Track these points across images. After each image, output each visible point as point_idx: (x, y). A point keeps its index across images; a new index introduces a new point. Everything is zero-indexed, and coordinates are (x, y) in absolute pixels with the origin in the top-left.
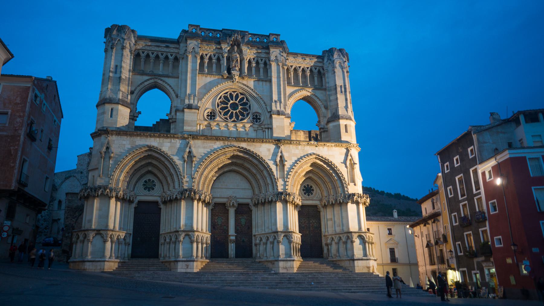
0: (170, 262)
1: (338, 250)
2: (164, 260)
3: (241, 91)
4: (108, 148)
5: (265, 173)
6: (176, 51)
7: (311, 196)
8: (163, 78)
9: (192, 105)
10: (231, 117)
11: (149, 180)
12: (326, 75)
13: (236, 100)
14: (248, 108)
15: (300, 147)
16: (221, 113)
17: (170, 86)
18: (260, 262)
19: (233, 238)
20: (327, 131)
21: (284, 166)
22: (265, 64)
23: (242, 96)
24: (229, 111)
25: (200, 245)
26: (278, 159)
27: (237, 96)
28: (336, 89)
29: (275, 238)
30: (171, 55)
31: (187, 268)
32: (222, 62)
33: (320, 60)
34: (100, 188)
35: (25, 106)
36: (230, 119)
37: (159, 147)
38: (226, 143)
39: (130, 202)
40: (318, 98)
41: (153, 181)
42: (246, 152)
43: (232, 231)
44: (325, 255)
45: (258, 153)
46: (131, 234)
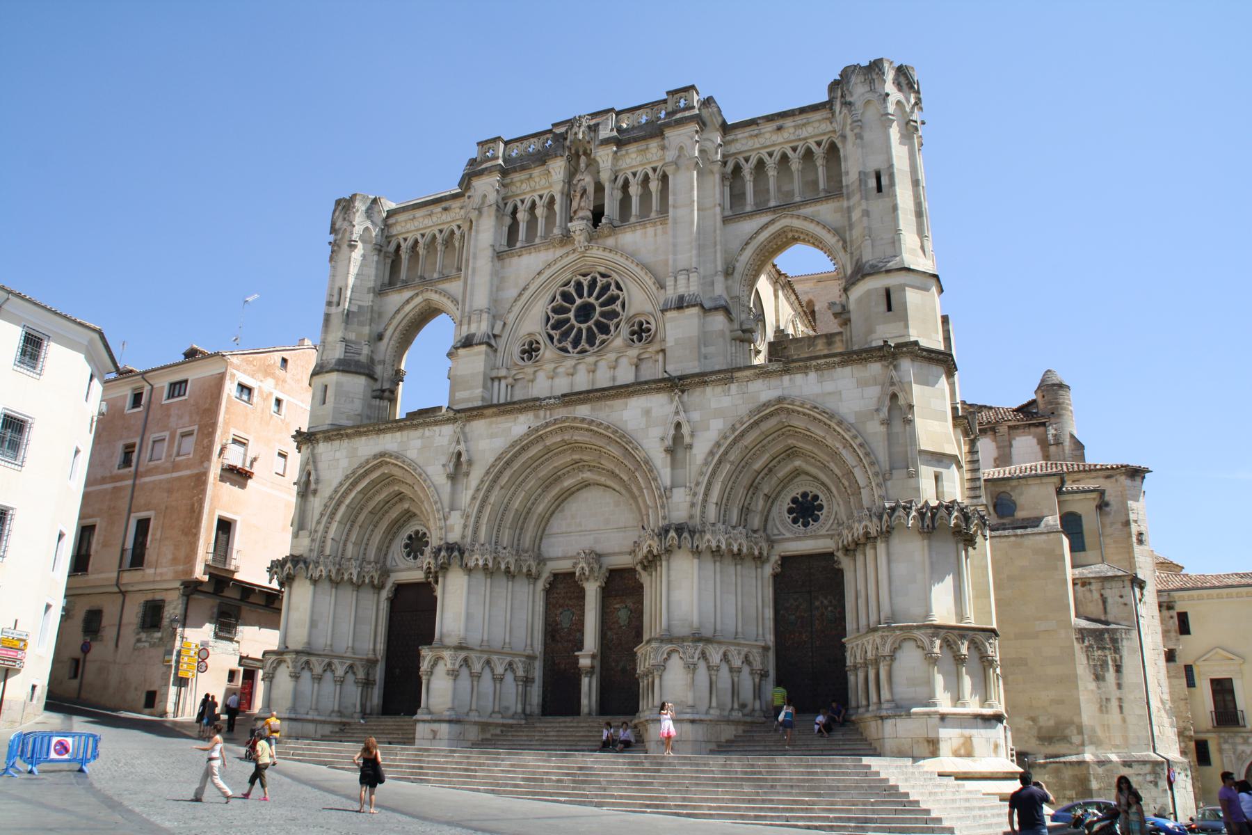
4: (309, 474)
7: (813, 526)
9: (474, 335)
10: (576, 343)
11: (417, 532)
13: (590, 295)
15: (734, 387)
16: (551, 338)
23: (605, 280)
24: (572, 327)
27: (593, 283)
36: (575, 347)
38: (542, 413)
42: (590, 426)
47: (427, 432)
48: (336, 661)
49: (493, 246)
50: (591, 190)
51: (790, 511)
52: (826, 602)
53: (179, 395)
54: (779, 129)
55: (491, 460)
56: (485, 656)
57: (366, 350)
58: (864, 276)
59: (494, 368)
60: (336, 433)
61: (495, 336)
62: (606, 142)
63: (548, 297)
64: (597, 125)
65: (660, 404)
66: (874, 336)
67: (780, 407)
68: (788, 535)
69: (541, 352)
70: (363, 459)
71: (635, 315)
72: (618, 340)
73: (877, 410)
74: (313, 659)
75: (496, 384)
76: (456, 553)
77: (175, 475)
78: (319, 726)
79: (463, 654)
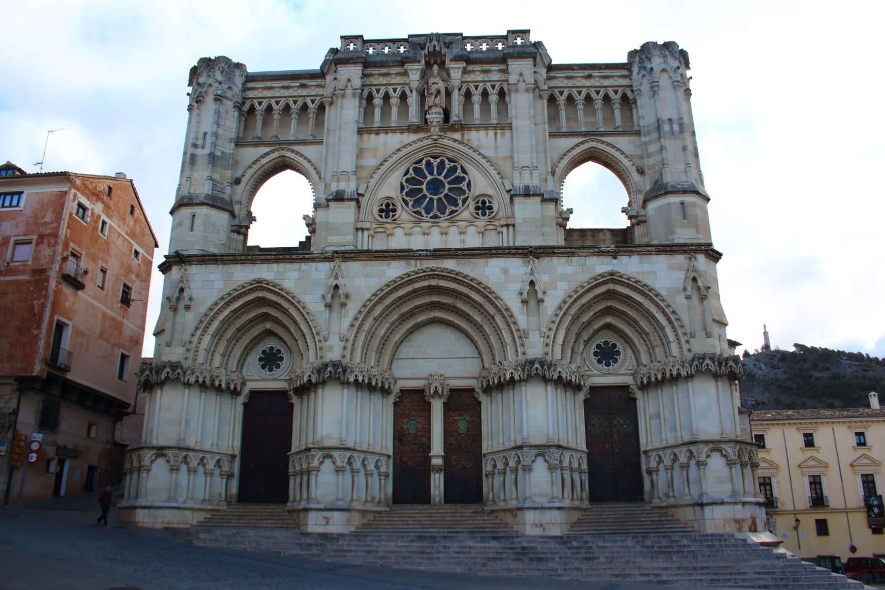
0: (299, 511)
1: (671, 485)
2: (290, 508)
3: (450, 154)
4: (182, 290)
5: (498, 318)
6: (319, 91)
7: (613, 367)
8: (295, 148)
9: (344, 191)
11: (272, 348)
12: (639, 102)
13: (439, 174)
14: (465, 188)
15: (575, 259)
16: (406, 203)
17: (309, 161)
18: (492, 512)
19: (437, 462)
20: (645, 222)
21: (540, 301)
22: (502, 94)
23: (452, 164)
24: (425, 196)
25: (361, 479)
26: (527, 288)
28: (659, 128)
29: (519, 462)
30: (313, 102)
31: (327, 524)
32: (409, 100)
33: (624, 72)
34: (165, 367)
35: (58, 227)
37: (277, 282)
38: (413, 262)
39: (235, 393)
40: (623, 153)
41: (279, 351)
42: (454, 277)
43: (437, 447)
44: (646, 496)
45: (481, 279)
46: (233, 457)
47: (303, 266)
48: (208, 456)
49: (358, 122)
50: (443, 92)
52: (621, 421)
53: (10, 206)
54: (589, 77)
55: (368, 295)
58: (667, 193)
59: (357, 220)
60: (207, 259)
61: (359, 194)
62: (457, 59)
63: (403, 169)
64: (451, 43)
65: (516, 266)
66: (675, 236)
67: (613, 278)
68: (596, 372)
69: (398, 213)
70: (239, 283)
71: (480, 195)
72: (467, 213)
73: (685, 289)
74: (191, 454)
75: (360, 233)
76: (340, 370)
77: (8, 278)
78: (196, 513)
79: (349, 454)
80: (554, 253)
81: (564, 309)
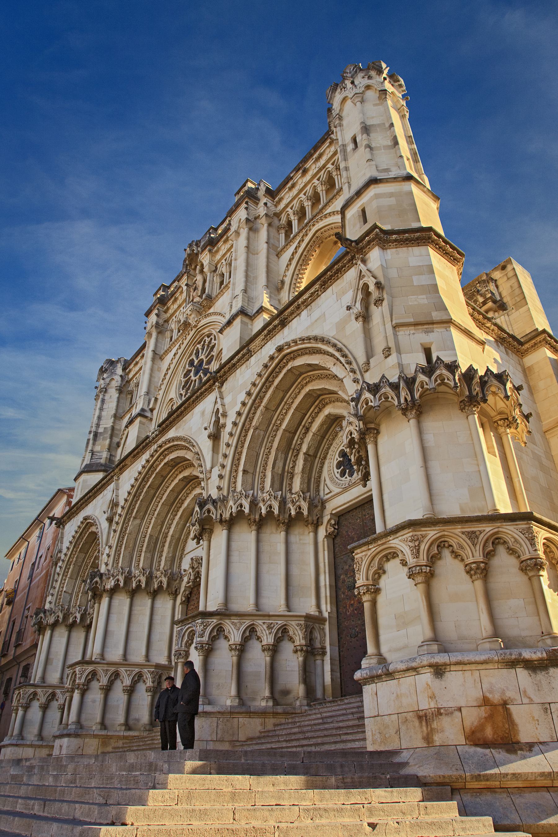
51: (339, 465)
56: (113, 669)
57: (105, 455)
76: (97, 579)
79: (90, 668)
80: (234, 365)
81: (240, 425)
